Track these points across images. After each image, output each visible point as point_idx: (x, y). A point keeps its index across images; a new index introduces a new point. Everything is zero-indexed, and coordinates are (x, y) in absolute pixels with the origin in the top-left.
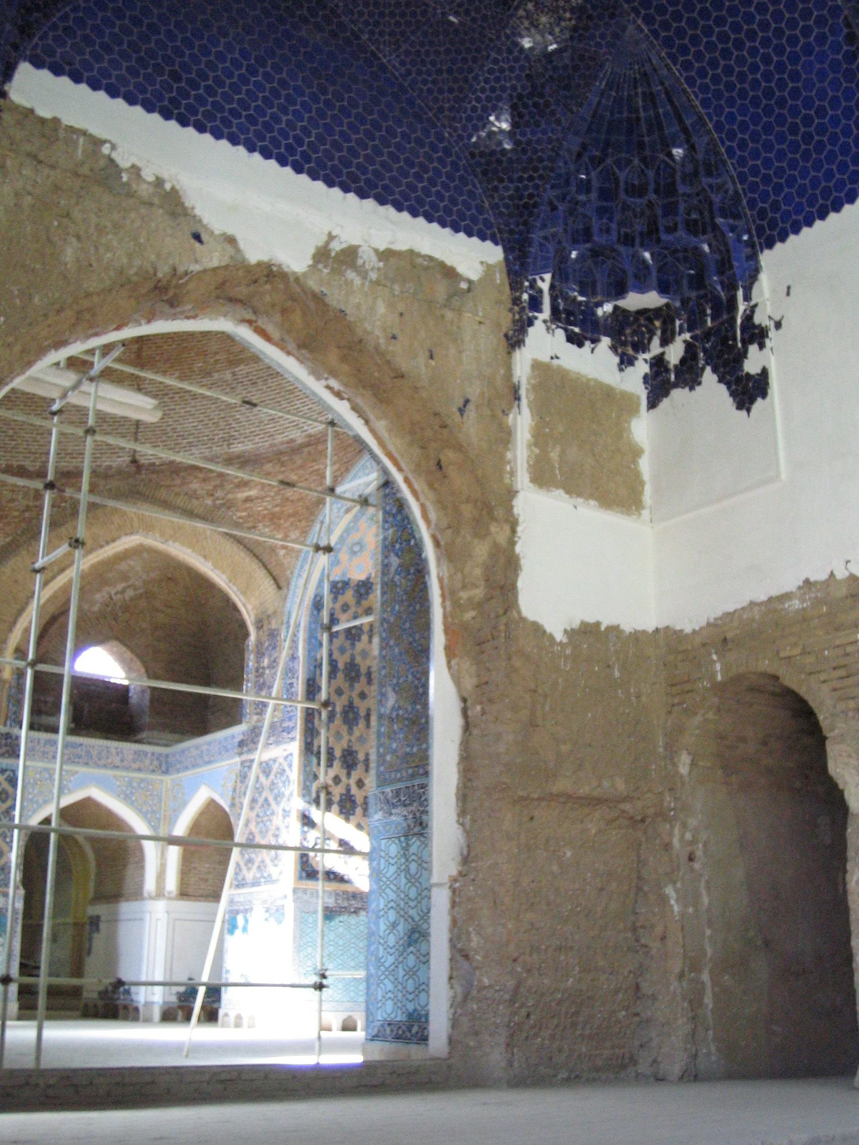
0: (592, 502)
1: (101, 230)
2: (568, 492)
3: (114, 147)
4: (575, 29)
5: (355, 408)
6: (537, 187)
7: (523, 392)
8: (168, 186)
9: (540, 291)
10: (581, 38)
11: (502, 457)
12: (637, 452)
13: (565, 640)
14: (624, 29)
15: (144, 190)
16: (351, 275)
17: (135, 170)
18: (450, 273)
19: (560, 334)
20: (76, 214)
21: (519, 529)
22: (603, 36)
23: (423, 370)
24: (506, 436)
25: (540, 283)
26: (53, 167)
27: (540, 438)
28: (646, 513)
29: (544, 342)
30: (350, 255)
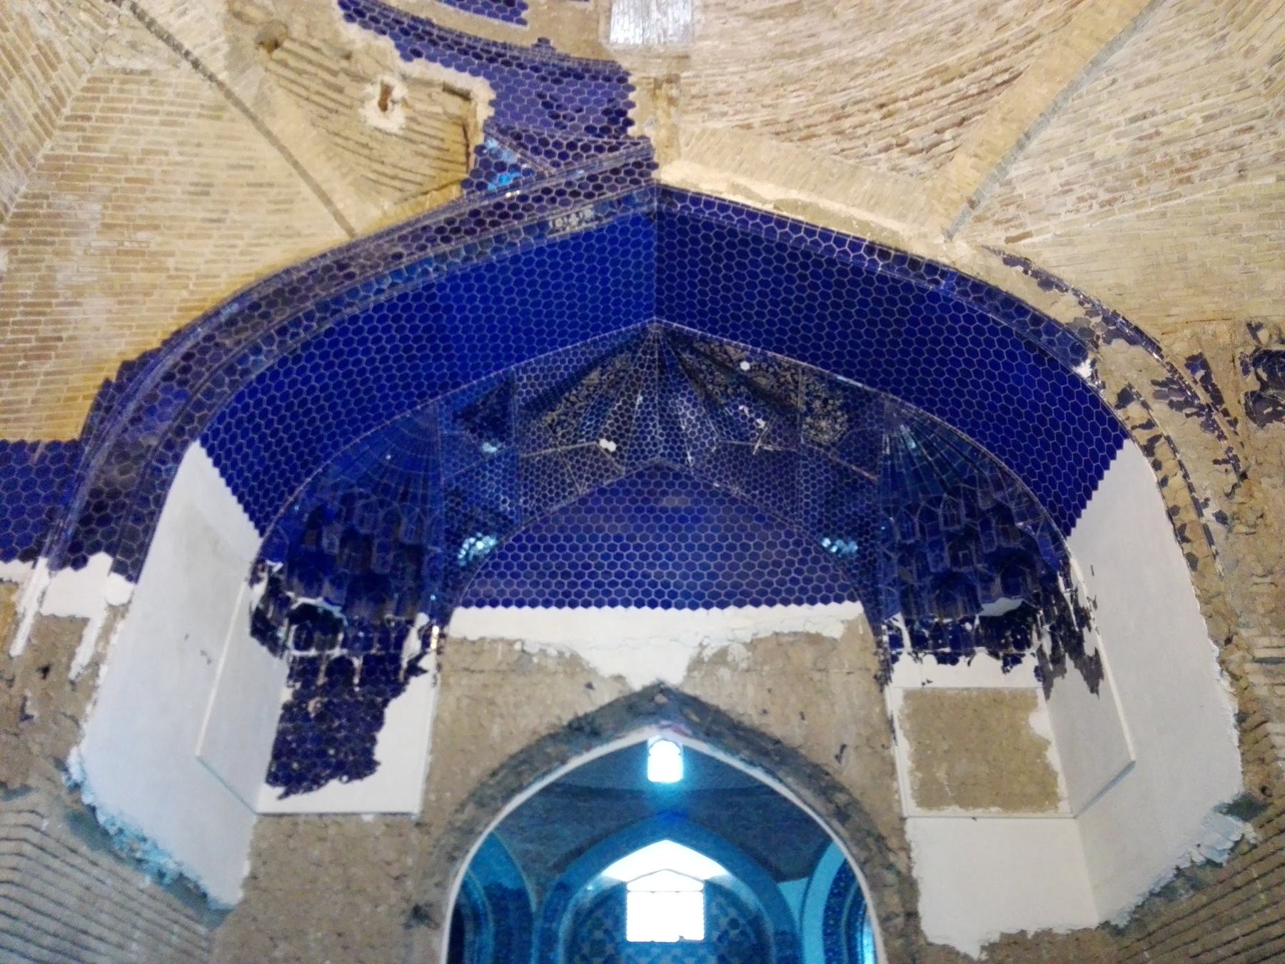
0: (994, 809)
1: (516, 705)
4: (849, 420)
5: (769, 772)
7: (896, 725)
8: (567, 655)
9: (899, 630)
10: (857, 424)
11: (888, 787)
12: (1042, 745)
13: (984, 957)
14: (882, 405)
15: (551, 664)
16: (724, 673)
17: (543, 652)
18: (814, 639)
19: (930, 659)
20: (499, 700)
21: (913, 855)
22: (871, 417)
26: (482, 672)
27: (922, 760)
29: (916, 671)
30: (721, 657)
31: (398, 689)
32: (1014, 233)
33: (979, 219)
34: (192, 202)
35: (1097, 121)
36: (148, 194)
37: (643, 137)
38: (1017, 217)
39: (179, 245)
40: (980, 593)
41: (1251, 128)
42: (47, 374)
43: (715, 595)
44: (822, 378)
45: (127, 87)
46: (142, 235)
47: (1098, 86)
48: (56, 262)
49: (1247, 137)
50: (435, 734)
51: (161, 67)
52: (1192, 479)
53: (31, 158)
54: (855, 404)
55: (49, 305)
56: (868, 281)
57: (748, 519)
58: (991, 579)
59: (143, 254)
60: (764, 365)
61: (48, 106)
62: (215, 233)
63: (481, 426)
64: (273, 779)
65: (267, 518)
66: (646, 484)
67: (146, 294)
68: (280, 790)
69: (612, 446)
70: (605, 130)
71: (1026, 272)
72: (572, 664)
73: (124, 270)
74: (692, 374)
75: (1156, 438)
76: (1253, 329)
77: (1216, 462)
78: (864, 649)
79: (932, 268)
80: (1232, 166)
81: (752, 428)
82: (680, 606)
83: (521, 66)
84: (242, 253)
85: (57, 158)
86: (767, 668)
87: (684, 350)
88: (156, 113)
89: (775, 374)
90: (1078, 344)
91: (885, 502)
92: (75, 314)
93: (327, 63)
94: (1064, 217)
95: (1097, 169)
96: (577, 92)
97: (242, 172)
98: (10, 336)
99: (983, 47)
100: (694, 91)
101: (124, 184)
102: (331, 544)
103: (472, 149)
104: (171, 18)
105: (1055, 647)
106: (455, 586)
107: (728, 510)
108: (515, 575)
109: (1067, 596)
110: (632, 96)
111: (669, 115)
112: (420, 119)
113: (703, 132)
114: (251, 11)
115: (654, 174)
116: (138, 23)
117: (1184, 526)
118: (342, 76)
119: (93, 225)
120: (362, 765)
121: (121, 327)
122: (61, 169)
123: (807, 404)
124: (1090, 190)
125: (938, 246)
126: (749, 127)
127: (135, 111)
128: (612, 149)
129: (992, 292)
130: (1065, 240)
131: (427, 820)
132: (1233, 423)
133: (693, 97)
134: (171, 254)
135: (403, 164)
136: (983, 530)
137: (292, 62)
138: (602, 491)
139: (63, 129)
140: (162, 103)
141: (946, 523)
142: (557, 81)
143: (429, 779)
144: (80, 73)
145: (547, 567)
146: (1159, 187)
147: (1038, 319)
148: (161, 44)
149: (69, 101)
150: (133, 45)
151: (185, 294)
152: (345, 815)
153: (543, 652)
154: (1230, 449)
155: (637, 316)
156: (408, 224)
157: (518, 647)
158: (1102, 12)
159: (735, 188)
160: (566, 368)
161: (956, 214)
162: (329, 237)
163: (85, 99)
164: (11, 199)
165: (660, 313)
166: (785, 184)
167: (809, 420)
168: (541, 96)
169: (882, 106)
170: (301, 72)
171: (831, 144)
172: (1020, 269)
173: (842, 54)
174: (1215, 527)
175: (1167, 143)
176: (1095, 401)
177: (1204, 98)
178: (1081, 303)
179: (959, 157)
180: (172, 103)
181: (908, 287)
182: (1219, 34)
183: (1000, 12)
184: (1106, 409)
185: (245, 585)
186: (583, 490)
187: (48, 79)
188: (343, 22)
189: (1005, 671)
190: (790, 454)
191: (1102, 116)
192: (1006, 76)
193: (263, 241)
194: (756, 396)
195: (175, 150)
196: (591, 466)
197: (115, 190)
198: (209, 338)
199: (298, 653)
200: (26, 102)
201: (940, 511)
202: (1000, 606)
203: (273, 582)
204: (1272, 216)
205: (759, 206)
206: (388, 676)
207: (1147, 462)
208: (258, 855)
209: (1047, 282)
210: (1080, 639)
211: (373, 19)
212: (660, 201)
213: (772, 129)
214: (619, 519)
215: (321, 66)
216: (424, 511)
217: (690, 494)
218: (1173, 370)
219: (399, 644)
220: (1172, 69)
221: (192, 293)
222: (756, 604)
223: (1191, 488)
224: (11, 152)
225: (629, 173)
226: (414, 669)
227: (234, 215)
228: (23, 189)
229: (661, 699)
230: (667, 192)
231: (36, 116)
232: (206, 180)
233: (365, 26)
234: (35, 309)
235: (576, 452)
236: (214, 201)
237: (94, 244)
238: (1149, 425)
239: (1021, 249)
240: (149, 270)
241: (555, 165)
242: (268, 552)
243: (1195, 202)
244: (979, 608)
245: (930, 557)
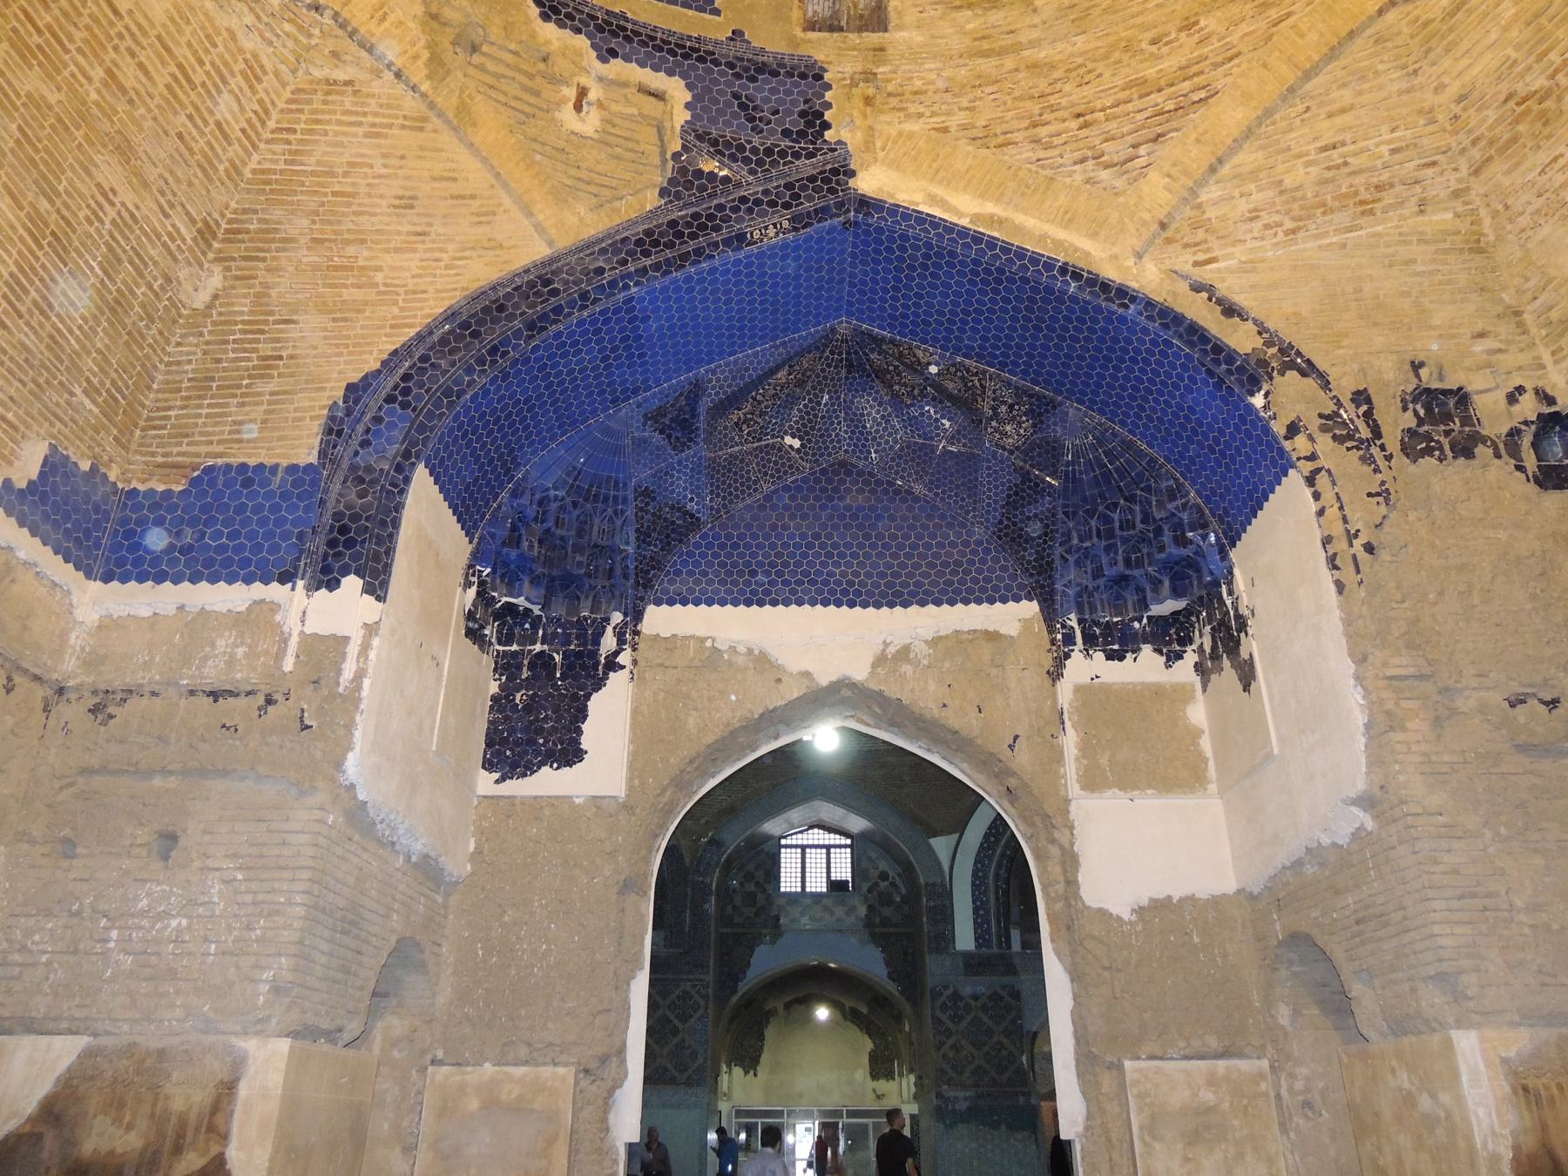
1: (710, 700)
2: (1123, 786)
3: (714, 640)
4: (1034, 425)
6: (1050, 547)
7: (1066, 717)
12: (1197, 734)
13: (1134, 918)
15: (740, 660)
16: (907, 668)
17: (733, 649)
18: (992, 636)
20: (694, 694)
24: (1058, 757)
27: (1087, 748)
28: (1213, 788)
30: (904, 653)
31: (599, 684)
32: (1201, 257)
33: (1169, 241)
35: (1289, 149)
36: (355, 208)
37: (840, 142)
38: (1205, 241)
39: (388, 260)
40: (1149, 595)
41: (1434, 163)
42: (272, 394)
43: (898, 594)
44: (1009, 384)
45: (330, 98)
46: (351, 250)
47: (1293, 112)
48: (270, 279)
49: (1430, 172)
50: (635, 725)
51: (363, 76)
52: (1347, 511)
53: (239, 173)
54: (1041, 410)
55: (266, 322)
56: (1060, 300)
57: (930, 517)
58: (1161, 582)
59: (351, 269)
60: (953, 370)
61: (255, 120)
62: (420, 246)
63: (670, 427)
64: (488, 765)
65: (476, 526)
66: (829, 481)
67: (359, 311)
68: (496, 776)
69: (796, 443)
70: (802, 134)
71: (1210, 299)
72: (761, 661)
73: (336, 286)
74: (880, 374)
75: (1319, 470)
76: (1416, 367)
77: (1369, 495)
79: (1122, 292)
80: (1414, 200)
81: (937, 428)
82: (865, 605)
83: (716, 63)
85: (263, 172)
86: (947, 665)
87: (872, 351)
88: (360, 124)
89: (963, 378)
90: (1252, 374)
91: (1064, 506)
92: (292, 332)
93: (525, 67)
94: (1249, 245)
95: (1284, 197)
96: (773, 91)
97: (445, 184)
98: (231, 355)
99: (1183, 61)
100: (890, 88)
101: (330, 198)
102: (531, 547)
103: (669, 156)
104: (372, 26)
105: (1214, 648)
106: (644, 585)
107: (910, 509)
108: (705, 574)
109: (1228, 602)
110: (828, 96)
111: (865, 117)
112: (616, 121)
113: (900, 134)
114: (448, 13)
115: (852, 183)
116: (340, 32)
117: (1335, 555)
118: (538, 79)
119: (303, 240)
120: (570, 754)
121: (337, 346)
122: (268, 182)
123: (994, 409)
124: (1276, 218)
125: (1128, 268)
126: (945, 130)
127: (339, 123)
128: (811, 155)
129: (1178, 319)
130: (1249, 267)
132: (1389, 458)
133: (889, 95)
134: (379, 269)
135: (599, 168)
136: (1156, 537)
137: (490, 66)
138: (787, 488)
139: (267, 142)
140: (365, 114)
141: (1121, 528)
142: (753, 79)
143: (631, 767)
144: (284, 85)
145: (734, 565)
146: (1342, 218)
147: (1218, 348)
148: (363, 54)
149: (275, 115)
150: (335, 54)
151: (396, 310)
152: (556, 797)
153: (733, 649)
154: (1383, 483)
155: (827, 318)
156: (609, 236)
157: (709, 643)
158: (1302, 36)
159: (933, 199)
160: (755, 369)
161: (1146, 234)
163: (291, 111)
164: (223, 216)
165: (850, 314)
166: (981, 196)
167: (994, 423)
168: (736, 96)
169: (1079, 116)
170: (498, 76)
171: (1027, 153)
172: (1205, 295)
173: (1041, 55)
174: (1363, 556)
175: (1354, 173)
176: (1267, 430)
177: (1393, 131)
178: (1260, 333)
179: (1153, 175)
180: (376, 114)
181: (1098, 309)
182: (1411, 69)
183: (1202, 23)
184: (1275, 438)
185: (460, 589)
186: (767, 488)
187: (254, 92)
188: (539, 21)
189: (1168, 667)
190: (973, 454)
191: (1293, 144)
192: (1202, 94)
193: (467, 254)
194: (942, 397)
195: (379, 162)
196: (776, 463)
197: (322, 204)
198: (424, 359)
199: (501, 648)
200: (234, 116)
201: (1116, 516)
202: (1167, 606)
203: (482, 583)
204: (1446, 252)
205: (955, 220)
206: (589, 672)
207: (1308, 492)
208: (480, 833)
209: (1230, 310)
210: (1238, 643)
211: (570, 17)
212: (857, 211)
213: (971, 133)
214: (804, 517)
215: (520, 71)
216: (616, 512)
217: (873, 492)
218: (1339, 404)
219: (597, 643)
220: (1365, 99)
221: (402, 309)
222: (938, 603)
223: (1345, 521)
224: (221, 168)
225: (826, 181)
226: (612, 665)
228: (233, 205)
229: (846, 693)
230: (865, 203)
231: (243, 131)
232: (407, 193)
233: (561, 24)
234: (255, 329)
235: (761, 449)
237: (305, 260)
238: (1312, 457)
239: (1207, 274)
240: (359, 286)
241: (752, 172)
242: (477, 557)
243: (1374, 235)
244: (1147, 608)
245: (1105, 560)
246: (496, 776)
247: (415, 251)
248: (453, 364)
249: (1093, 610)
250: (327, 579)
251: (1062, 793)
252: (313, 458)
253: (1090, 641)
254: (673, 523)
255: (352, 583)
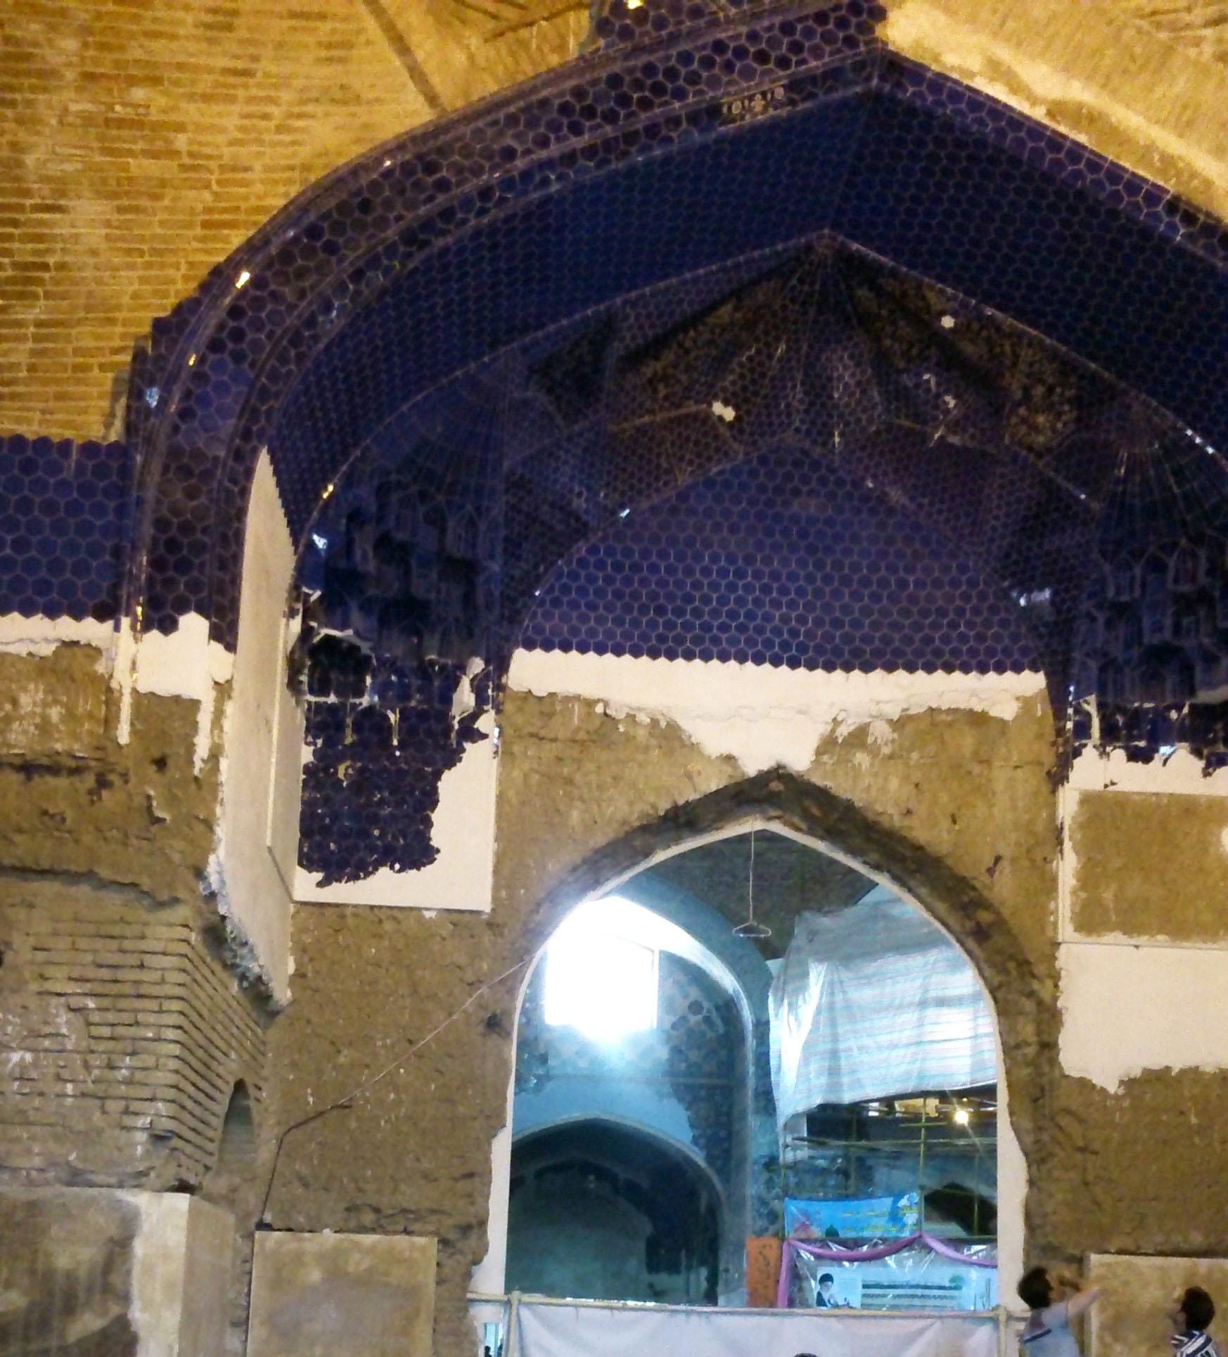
9: (1088, 715)
23: (945, 836)
25: (1086, 706)
34: (210, 41)
42: (39, 324)
43: (857, 653)
78: (1040, 736)
84: (279, 129)
131: (499, 920)
162: (402, 113)
216: (478, 509)
227: (267, 65)
236: (241, 42)
246: (318, 876)
247: (232, 99)
248: (302, 294)
249: (1119, 691)
250: (162, 620)
251: (1050, 933)
252: (115, 433)
253: (1110, 735)
254: (551, 528)
255: (193, 625)
